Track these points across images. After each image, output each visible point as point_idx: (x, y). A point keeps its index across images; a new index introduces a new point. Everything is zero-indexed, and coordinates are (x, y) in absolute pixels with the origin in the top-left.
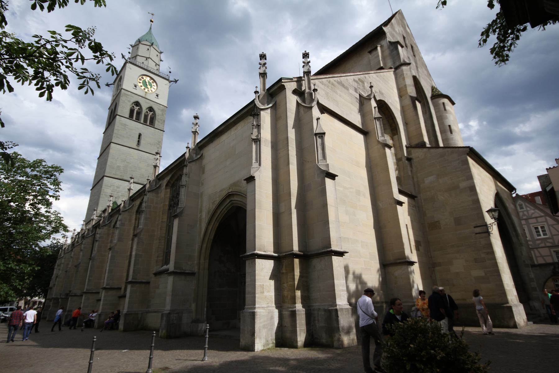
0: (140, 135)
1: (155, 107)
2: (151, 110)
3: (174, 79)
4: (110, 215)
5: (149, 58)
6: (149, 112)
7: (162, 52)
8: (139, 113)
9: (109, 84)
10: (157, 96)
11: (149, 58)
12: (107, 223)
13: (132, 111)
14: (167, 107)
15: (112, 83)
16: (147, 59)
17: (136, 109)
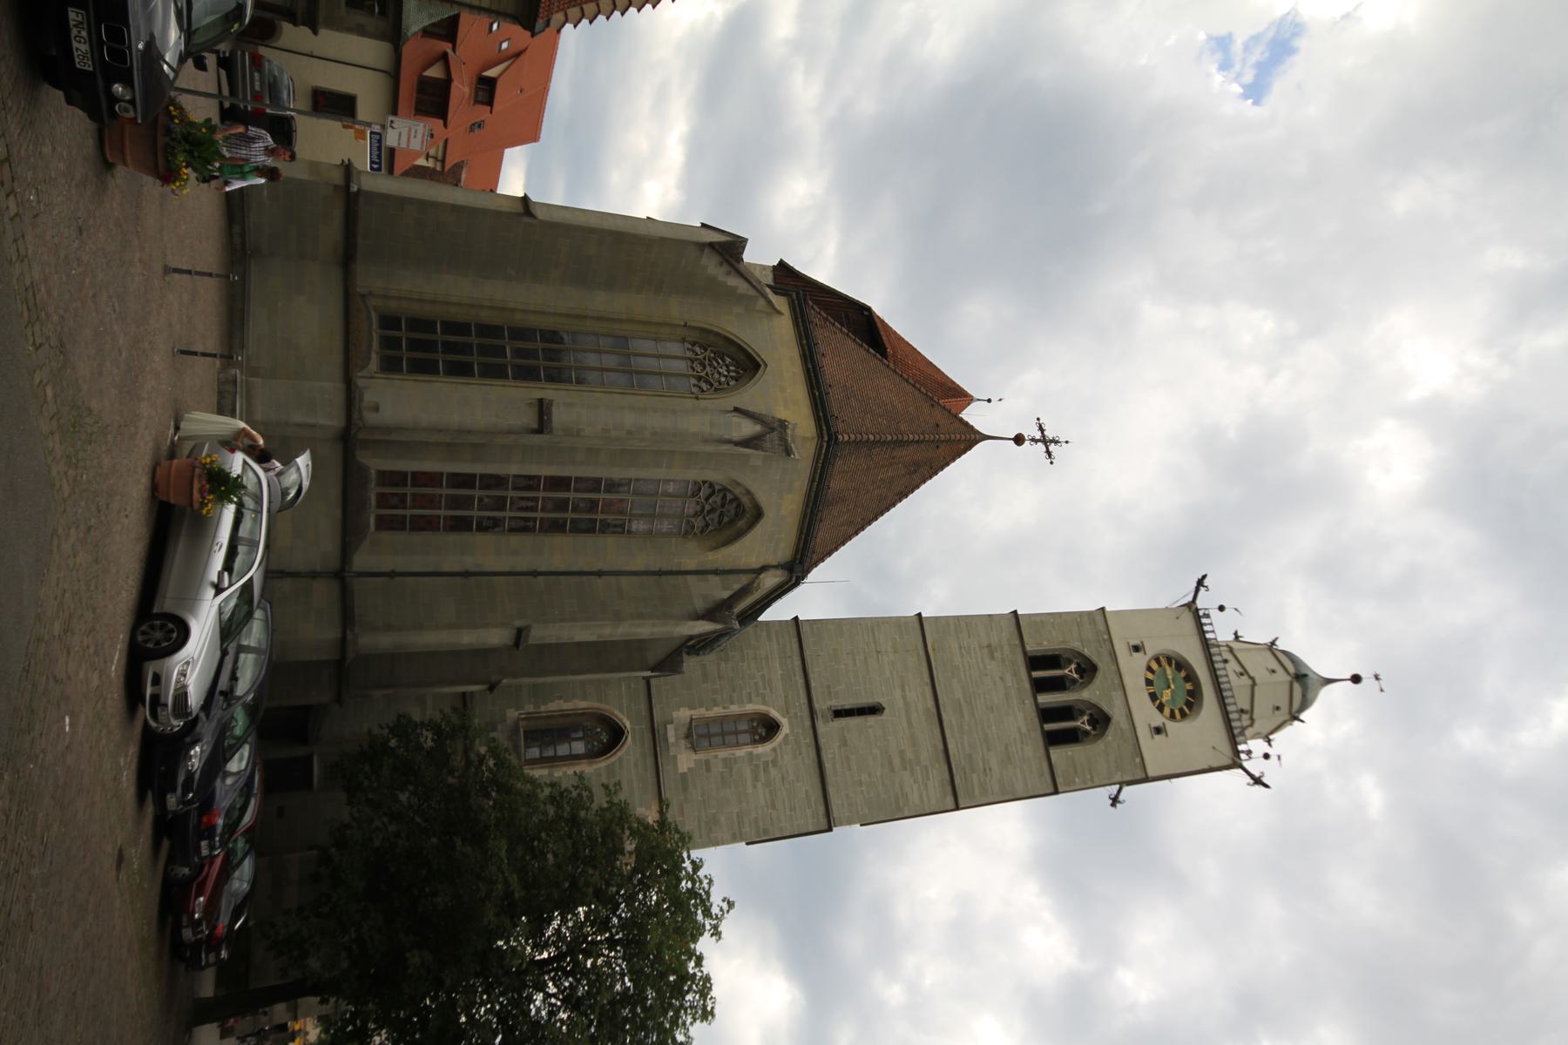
8: (1058, 685)
11: (1252, 678)
16: (1242, 674)
17: (1070, 671)
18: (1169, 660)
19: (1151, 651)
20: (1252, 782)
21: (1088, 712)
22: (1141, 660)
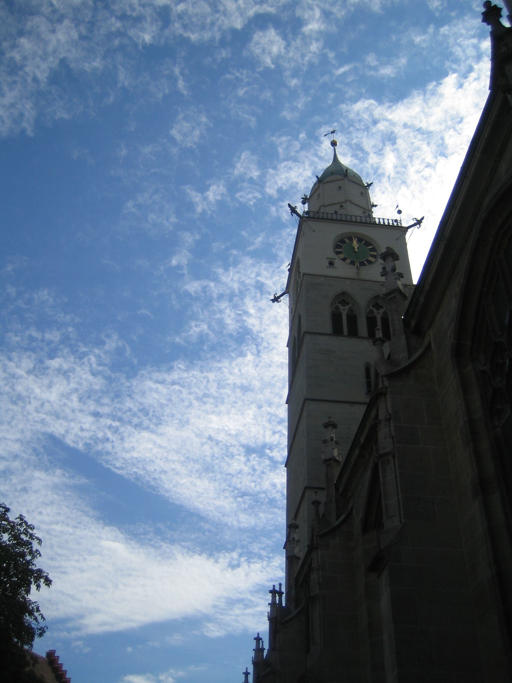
2: (380, 304)
3: (413, 219)
4: (341, 489)
5: (346, 202)
6: (375, 310)
7: (369, 183)
8: (352, 319)
9: (278, 295)
12: (337, 523)
13: (336, 317)
16: (342, 206)
17: (344, 311)
18: (337, 246)
19: (333, 255)
20: (418, 226)
21: (371, 307)
22: (338, 262)
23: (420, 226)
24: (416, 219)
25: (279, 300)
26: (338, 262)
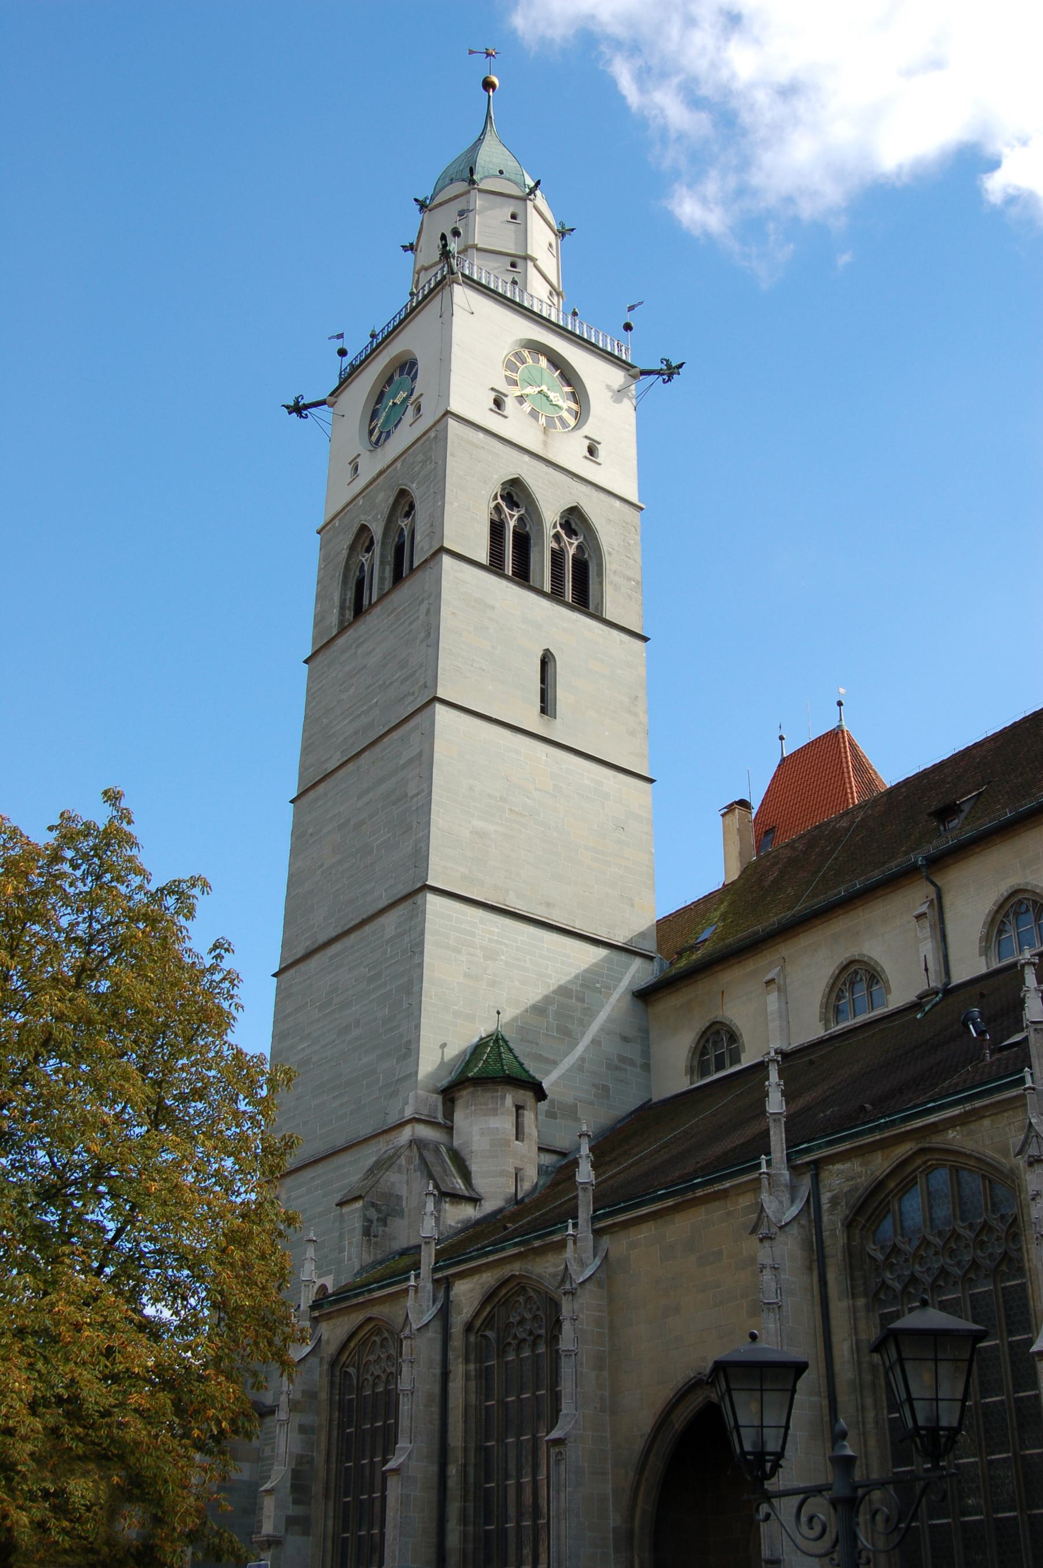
0: (546, 661)
1: (596, 509)
2: (574, 526)
8: (523, 542)
10: (592, 451)
14: (642, 509)
15: (323, 395)
23: (669, 380)
24: (667, 361)
25: (305, 412)
26: (510, 403)
